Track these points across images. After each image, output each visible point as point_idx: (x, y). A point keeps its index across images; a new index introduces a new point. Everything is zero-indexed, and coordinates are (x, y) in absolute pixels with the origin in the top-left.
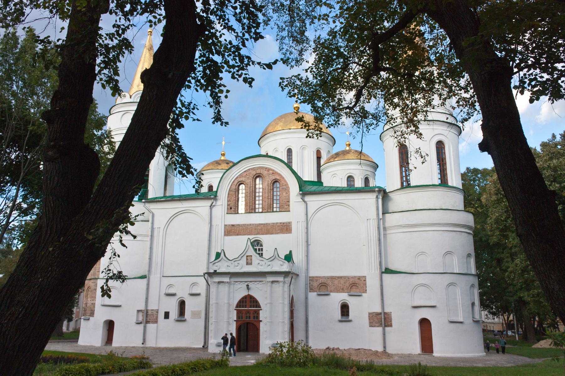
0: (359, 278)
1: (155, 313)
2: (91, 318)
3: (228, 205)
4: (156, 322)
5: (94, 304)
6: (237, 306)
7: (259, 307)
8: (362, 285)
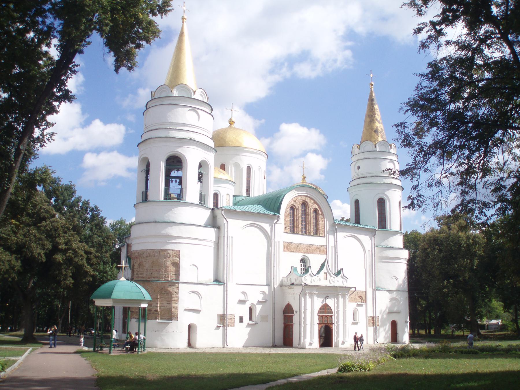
0: (362, 292)
1: (233, 317)
2: (173, 322)
3: (285, 224)
4: (233, 325)
5: (177, 308)
6: (318, 313)
7: (331, 312)
8: (364, 298)
